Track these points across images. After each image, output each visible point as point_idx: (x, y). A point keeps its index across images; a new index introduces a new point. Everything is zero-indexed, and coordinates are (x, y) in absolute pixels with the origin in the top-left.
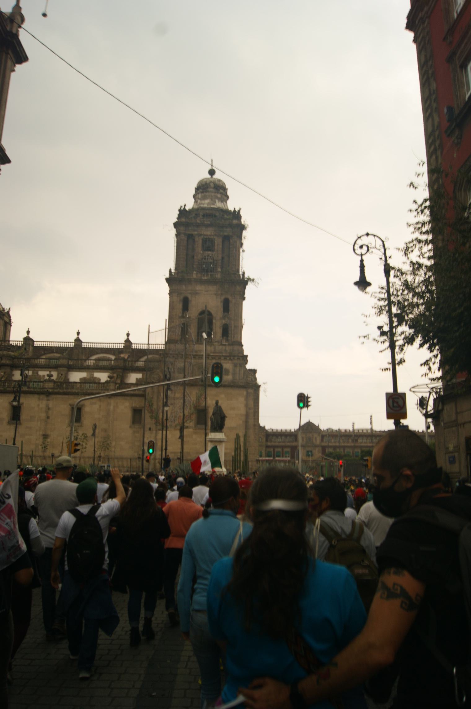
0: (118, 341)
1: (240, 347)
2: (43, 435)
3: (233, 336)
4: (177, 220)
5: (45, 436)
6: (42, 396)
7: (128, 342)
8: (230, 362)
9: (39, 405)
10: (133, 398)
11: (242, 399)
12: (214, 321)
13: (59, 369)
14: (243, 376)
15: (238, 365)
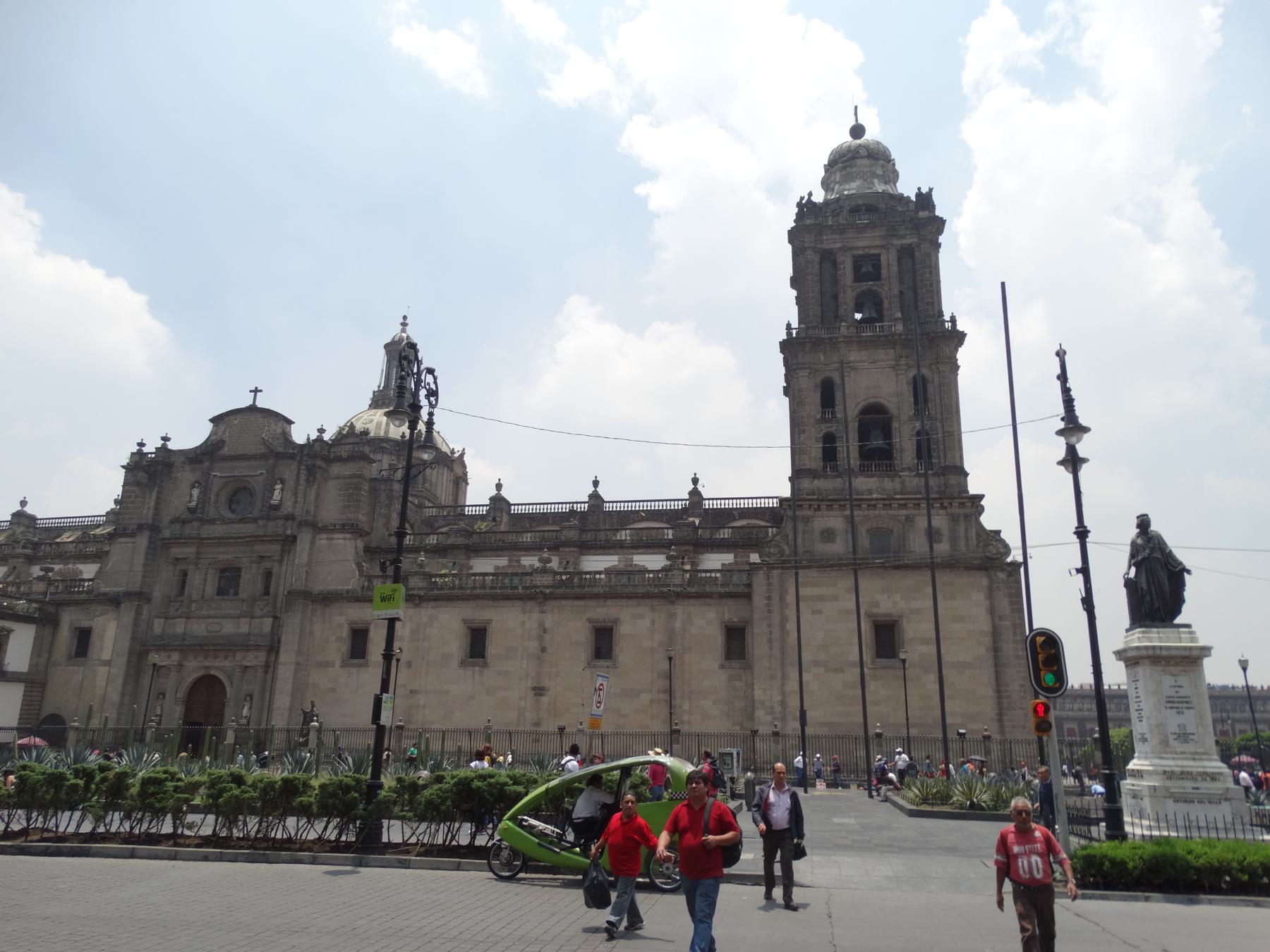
0: (675, 491)
1: (962, 478)
2: (534, 689)
3: (942, 456)
4: (794, 224)
5: (539, 691)
6: (530, 604)
7: (695, 493)
8: (941, 512)
9: (523, 623)
10: (724, 601)
11: (979, 597)
12: (895, 425)
13: (561, 549)
14: (975, 543)
15: (962, 518)
